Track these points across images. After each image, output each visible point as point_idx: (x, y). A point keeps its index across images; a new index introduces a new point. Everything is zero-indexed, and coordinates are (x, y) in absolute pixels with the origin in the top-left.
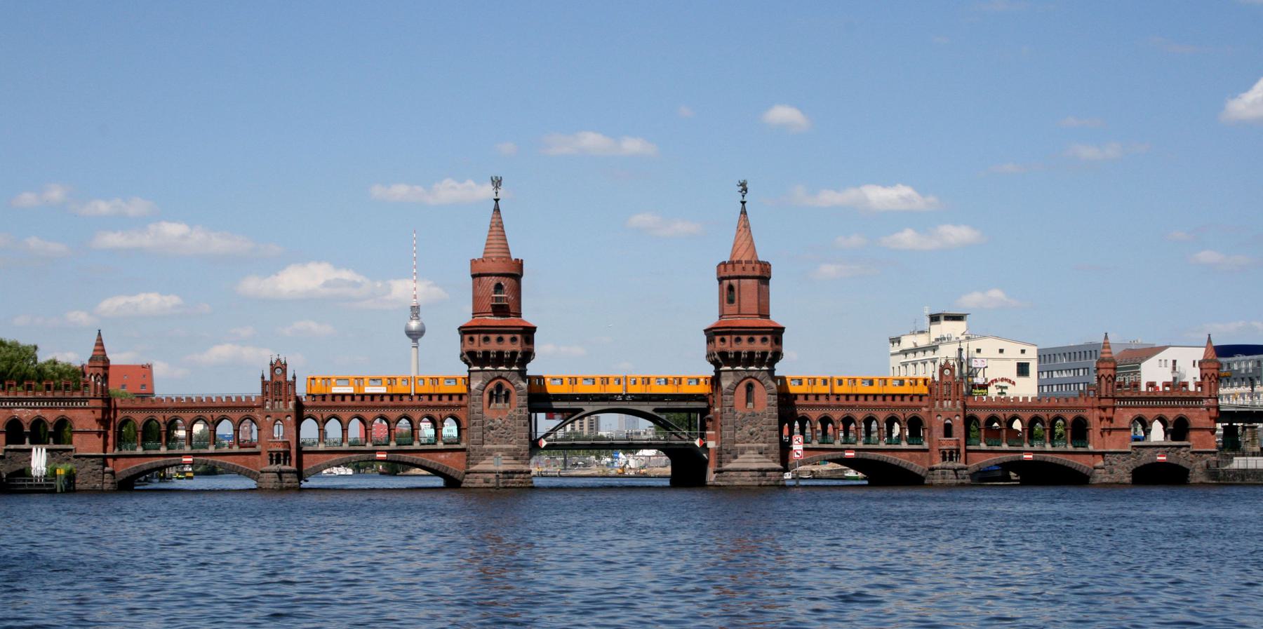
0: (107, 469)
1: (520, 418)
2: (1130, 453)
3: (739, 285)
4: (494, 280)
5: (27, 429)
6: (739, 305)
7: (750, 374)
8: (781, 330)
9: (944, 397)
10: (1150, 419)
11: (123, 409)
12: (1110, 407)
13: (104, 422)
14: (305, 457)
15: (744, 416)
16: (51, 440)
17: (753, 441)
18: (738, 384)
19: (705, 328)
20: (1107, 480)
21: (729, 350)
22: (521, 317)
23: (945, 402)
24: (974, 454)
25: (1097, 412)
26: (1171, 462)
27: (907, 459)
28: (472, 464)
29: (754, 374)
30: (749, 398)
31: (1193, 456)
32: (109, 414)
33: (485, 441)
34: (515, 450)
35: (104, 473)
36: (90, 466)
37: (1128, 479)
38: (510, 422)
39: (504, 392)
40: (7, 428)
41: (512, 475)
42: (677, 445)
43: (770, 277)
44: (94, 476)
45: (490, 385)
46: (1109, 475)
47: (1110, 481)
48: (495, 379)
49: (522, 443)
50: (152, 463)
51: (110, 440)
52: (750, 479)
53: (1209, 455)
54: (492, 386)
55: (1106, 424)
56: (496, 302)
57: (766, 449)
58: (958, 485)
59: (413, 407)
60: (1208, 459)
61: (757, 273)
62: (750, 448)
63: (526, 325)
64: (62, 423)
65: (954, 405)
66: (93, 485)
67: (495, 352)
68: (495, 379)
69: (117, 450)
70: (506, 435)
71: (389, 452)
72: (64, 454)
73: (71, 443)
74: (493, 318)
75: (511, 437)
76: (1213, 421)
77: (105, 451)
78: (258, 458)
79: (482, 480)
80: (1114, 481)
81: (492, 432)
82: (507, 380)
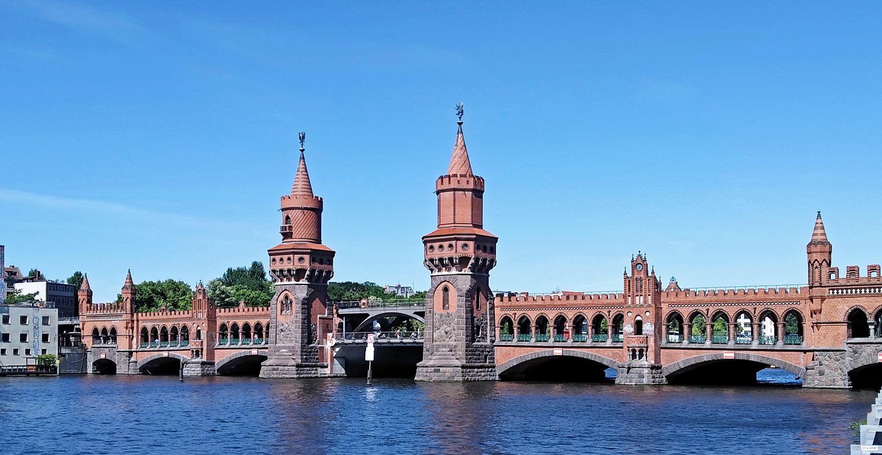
9: (635, 294)
15: (441, 316)
17: (447, 340)
27: (610, 357)
29: (447, 278)
30: (445, 301)
34: (293, 347)
35: (129, 363)
37: (843, 382)
46: (819, 377)
57: (455, 347)
62: (444, 346)
64: (114, 331)
65: (645, 302)
77: (130, 346)
81: (282, 333)
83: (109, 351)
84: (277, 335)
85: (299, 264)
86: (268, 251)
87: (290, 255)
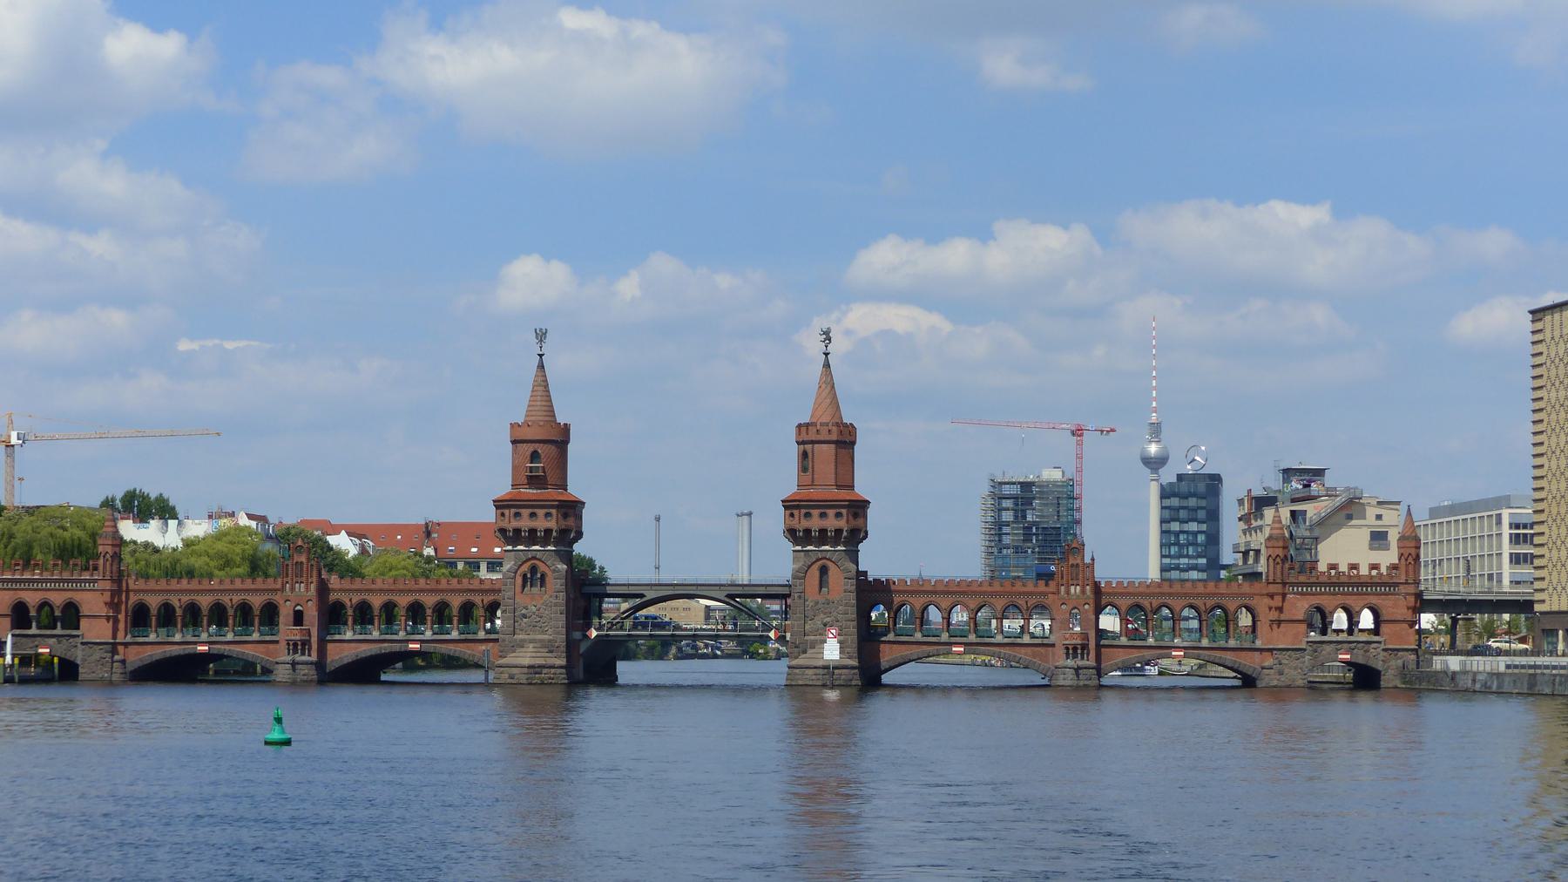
0: (116, 657)
2: (1305, 650)
3: (813, 451)
4: (530, 448)
5: (33, 613)
6: (813, 475)
7: (824, 554)
8: (864, 504)
9: (1071, 582)
10: (1331, 609)
11: (136, 591)
12: (1277, 594)
13: (114, 605)
14: (330, 646)
15: (817, 603)
16: (59, 624)
18: (809, 567)
19: (783, 498)
20: (1275, 683)
21: (797, 526)
22: (566, 490)
23: (1072, 588)
24: (1112, 650)
25: (1267, 601)
26: (1357, 661)
28: (501, 657)
30: (822, 583)
31: (1385, 654)
32: (120, 596)
33: (517, 631)
34: (550, 641)
35: (113, 662)
36: (98, 653)
39: (539, 575)
40: (12, 611)
41: (539, 670)
42: (613, 636)
43: (853, 443)
44: (102, 665)
46: (1278, 677)
47: (1280, 684)
49: (558, 633)
50: (165, 652)
51: (121, 626)
52: (814, 677)
53: (1406, 653)
54: (525, 568)
55: (1274, 615)
56: (531, 472)
58: (1077, 688)
59: (453, 591)
60: (1405, 658)
61: (834, 437)
63: (574, 499)
65: (1083, 592)
66: (101, 676)
69: (129, 636)
72: (71, 640)
73: (78, 628)
74: (528, 491)
76: (1410, 611)
77: (114, 637)
78: (277, 646)
79: (507, 676)
80: (1283, 684)
82: (543, 562)
83: (59, 642)
86: (494, 501)
87: (551, 510)
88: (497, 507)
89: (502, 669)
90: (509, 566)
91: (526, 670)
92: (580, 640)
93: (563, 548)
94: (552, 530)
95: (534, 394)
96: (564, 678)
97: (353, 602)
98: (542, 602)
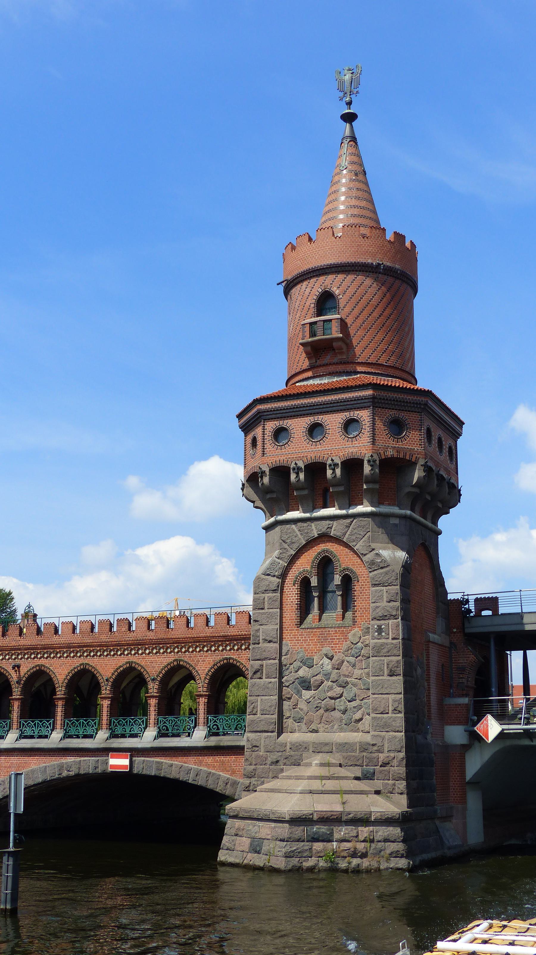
1: (378, 651)
28: (248, 789)
33: (289, 723)
34: (364, 747)
38: (354, 666)
39: (337, 580)
41: (323, 829)
45: (299, 562)
48: (311, 543)
49: (386, 727)
67: (301, 464)
68: (311, 543)
70: (340, 704)
71: (133, 752)
74: (311, 382)
75: (359, 707)
79: (244, 843)
81: (307, 694)
84: (286, 705)
85: (392, 443)
86: (240, 416)
88: (246, 428)
89: (238, 823)
90: (268, 562)
91: (284, 830)
92: (466, 748)
93: (396, 510)
94: (362, 461)
95: (334, 188)
96: (395, 855)
97: (22, 674)
98: (345, 645)
